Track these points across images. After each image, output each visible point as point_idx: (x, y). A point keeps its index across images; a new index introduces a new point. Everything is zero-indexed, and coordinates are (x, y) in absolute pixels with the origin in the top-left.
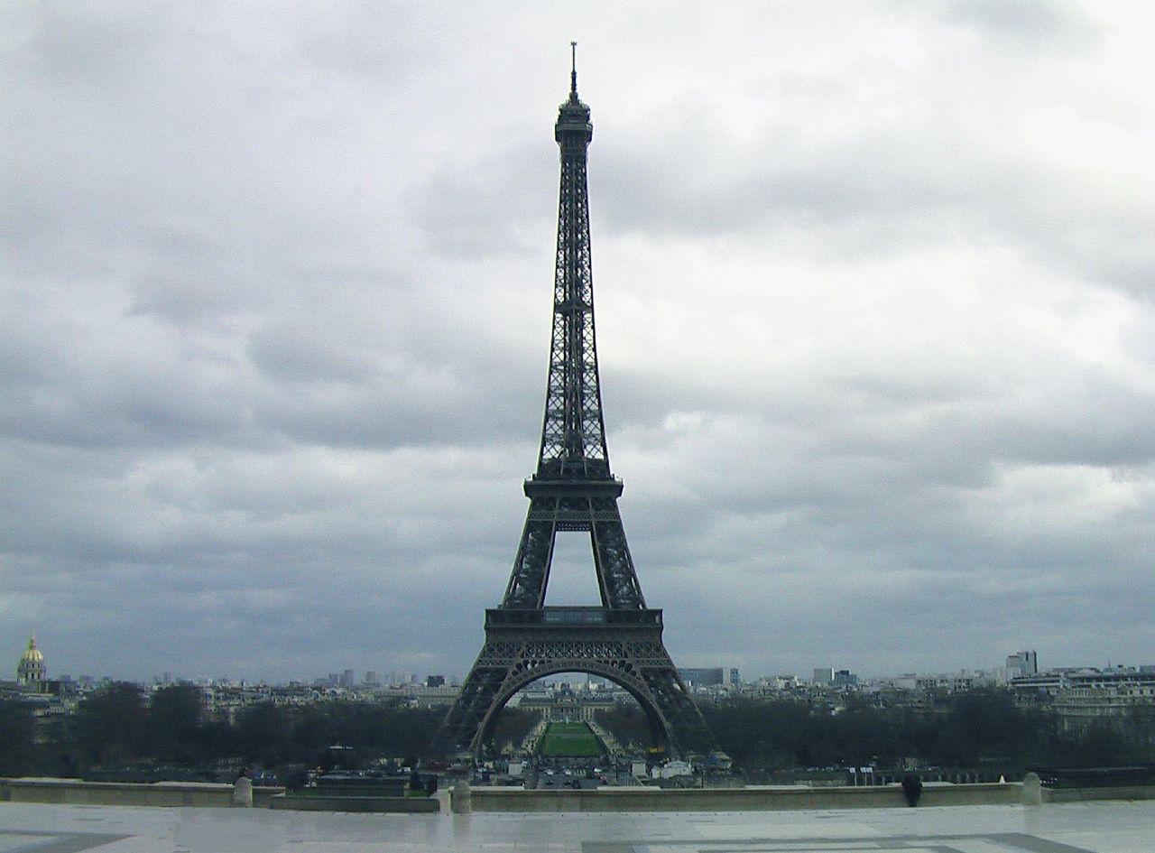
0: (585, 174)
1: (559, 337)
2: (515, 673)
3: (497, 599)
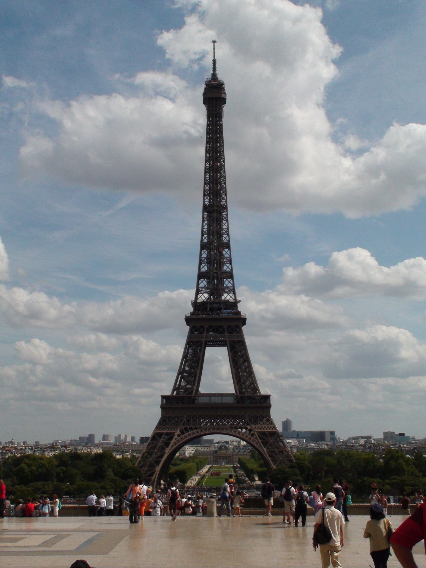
0: (221, 125)
1: (206, 227)
2: (179, 435)
3: (168, 390)
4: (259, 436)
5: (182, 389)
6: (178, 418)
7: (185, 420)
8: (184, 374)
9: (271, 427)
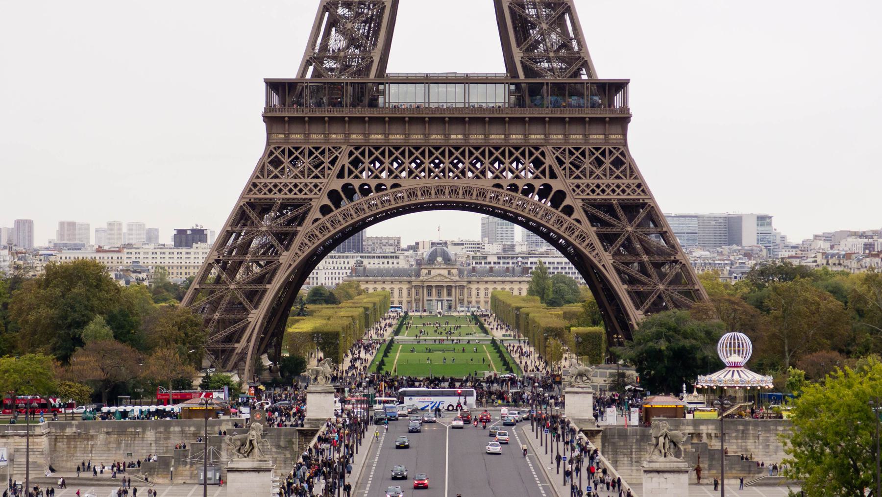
2: (325, 210)
5: (335, 58)
6: (323, 153)
8: (341, 11)
9: (628, 186)
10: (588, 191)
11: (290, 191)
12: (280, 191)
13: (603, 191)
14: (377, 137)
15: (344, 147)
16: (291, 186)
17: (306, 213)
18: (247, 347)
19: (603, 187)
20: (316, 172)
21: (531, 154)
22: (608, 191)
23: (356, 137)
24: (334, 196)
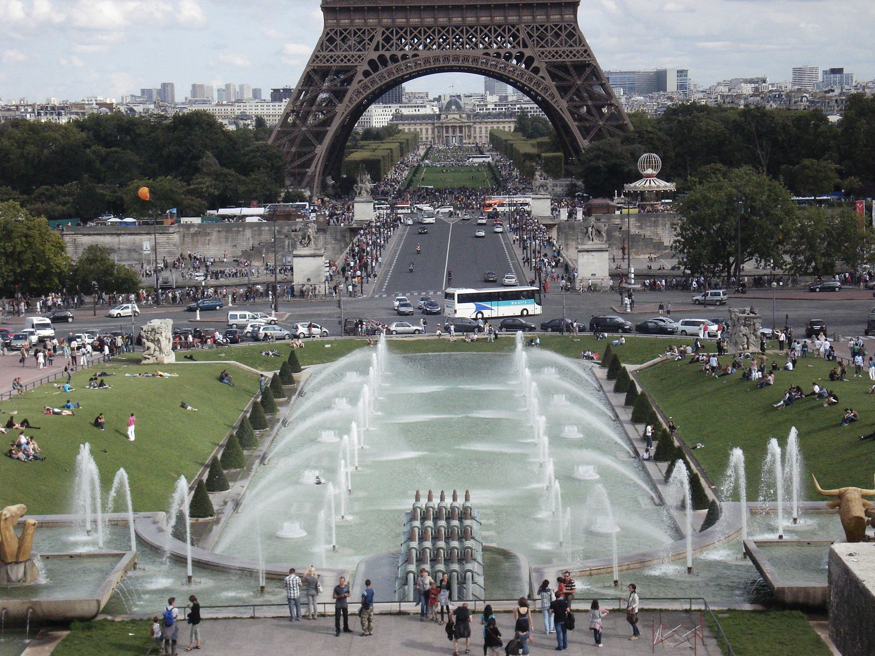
2: (366, 74)
4: (549, 72)
6: (364, 33)
7: (379, 38)
10: (550, 56)
11: (342, 60)
12: (335, 60)
13: (560, 56)
14: (401, 21)
15: (378, 29)
16: (342, 57)
17: (353, 76)
18: (315, 171)
19: (560, 53)
20: (360, 47)
21: (510, 30)
22: (564, 56)
23: (386, 21)
24: (371, 63)
